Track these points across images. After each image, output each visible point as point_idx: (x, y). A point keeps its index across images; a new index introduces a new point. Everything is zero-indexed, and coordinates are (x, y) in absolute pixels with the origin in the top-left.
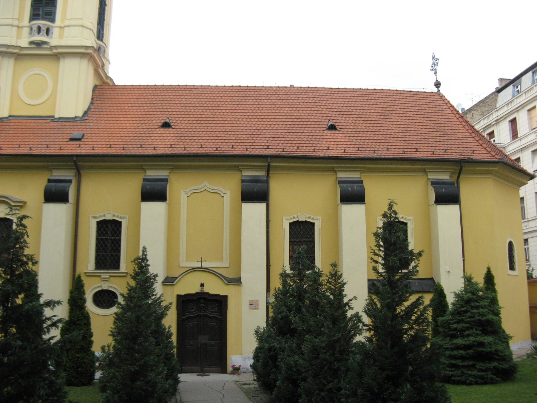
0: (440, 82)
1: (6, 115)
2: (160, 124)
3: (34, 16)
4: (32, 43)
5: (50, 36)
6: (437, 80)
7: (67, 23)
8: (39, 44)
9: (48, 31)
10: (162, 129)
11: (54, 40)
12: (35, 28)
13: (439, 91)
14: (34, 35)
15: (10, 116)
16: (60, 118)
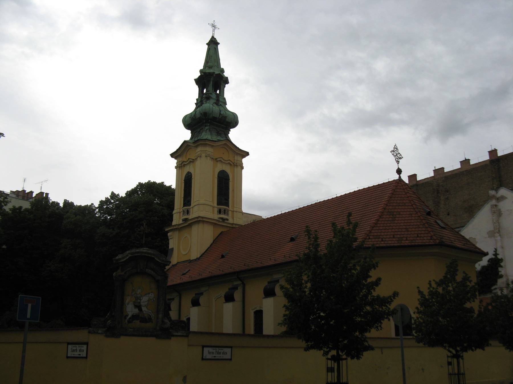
0: (401, 170)
1: (176, 263)
2: (221, 257)
3: (185, 205)
4: (183, 220)
5: (189, 214)
6: (399, 168)
7: (195, 204)
8: (185, 220)
9: (188, 212)
10: (221, 259)
11: (190, 217)
12: (186, 211)
13: (400, 177)
14: (185, 215)
15: (177, 263)
16: (192, 260)
